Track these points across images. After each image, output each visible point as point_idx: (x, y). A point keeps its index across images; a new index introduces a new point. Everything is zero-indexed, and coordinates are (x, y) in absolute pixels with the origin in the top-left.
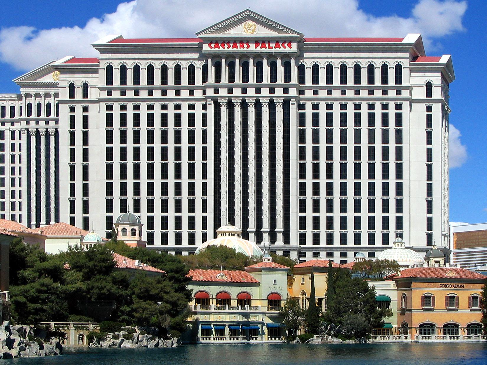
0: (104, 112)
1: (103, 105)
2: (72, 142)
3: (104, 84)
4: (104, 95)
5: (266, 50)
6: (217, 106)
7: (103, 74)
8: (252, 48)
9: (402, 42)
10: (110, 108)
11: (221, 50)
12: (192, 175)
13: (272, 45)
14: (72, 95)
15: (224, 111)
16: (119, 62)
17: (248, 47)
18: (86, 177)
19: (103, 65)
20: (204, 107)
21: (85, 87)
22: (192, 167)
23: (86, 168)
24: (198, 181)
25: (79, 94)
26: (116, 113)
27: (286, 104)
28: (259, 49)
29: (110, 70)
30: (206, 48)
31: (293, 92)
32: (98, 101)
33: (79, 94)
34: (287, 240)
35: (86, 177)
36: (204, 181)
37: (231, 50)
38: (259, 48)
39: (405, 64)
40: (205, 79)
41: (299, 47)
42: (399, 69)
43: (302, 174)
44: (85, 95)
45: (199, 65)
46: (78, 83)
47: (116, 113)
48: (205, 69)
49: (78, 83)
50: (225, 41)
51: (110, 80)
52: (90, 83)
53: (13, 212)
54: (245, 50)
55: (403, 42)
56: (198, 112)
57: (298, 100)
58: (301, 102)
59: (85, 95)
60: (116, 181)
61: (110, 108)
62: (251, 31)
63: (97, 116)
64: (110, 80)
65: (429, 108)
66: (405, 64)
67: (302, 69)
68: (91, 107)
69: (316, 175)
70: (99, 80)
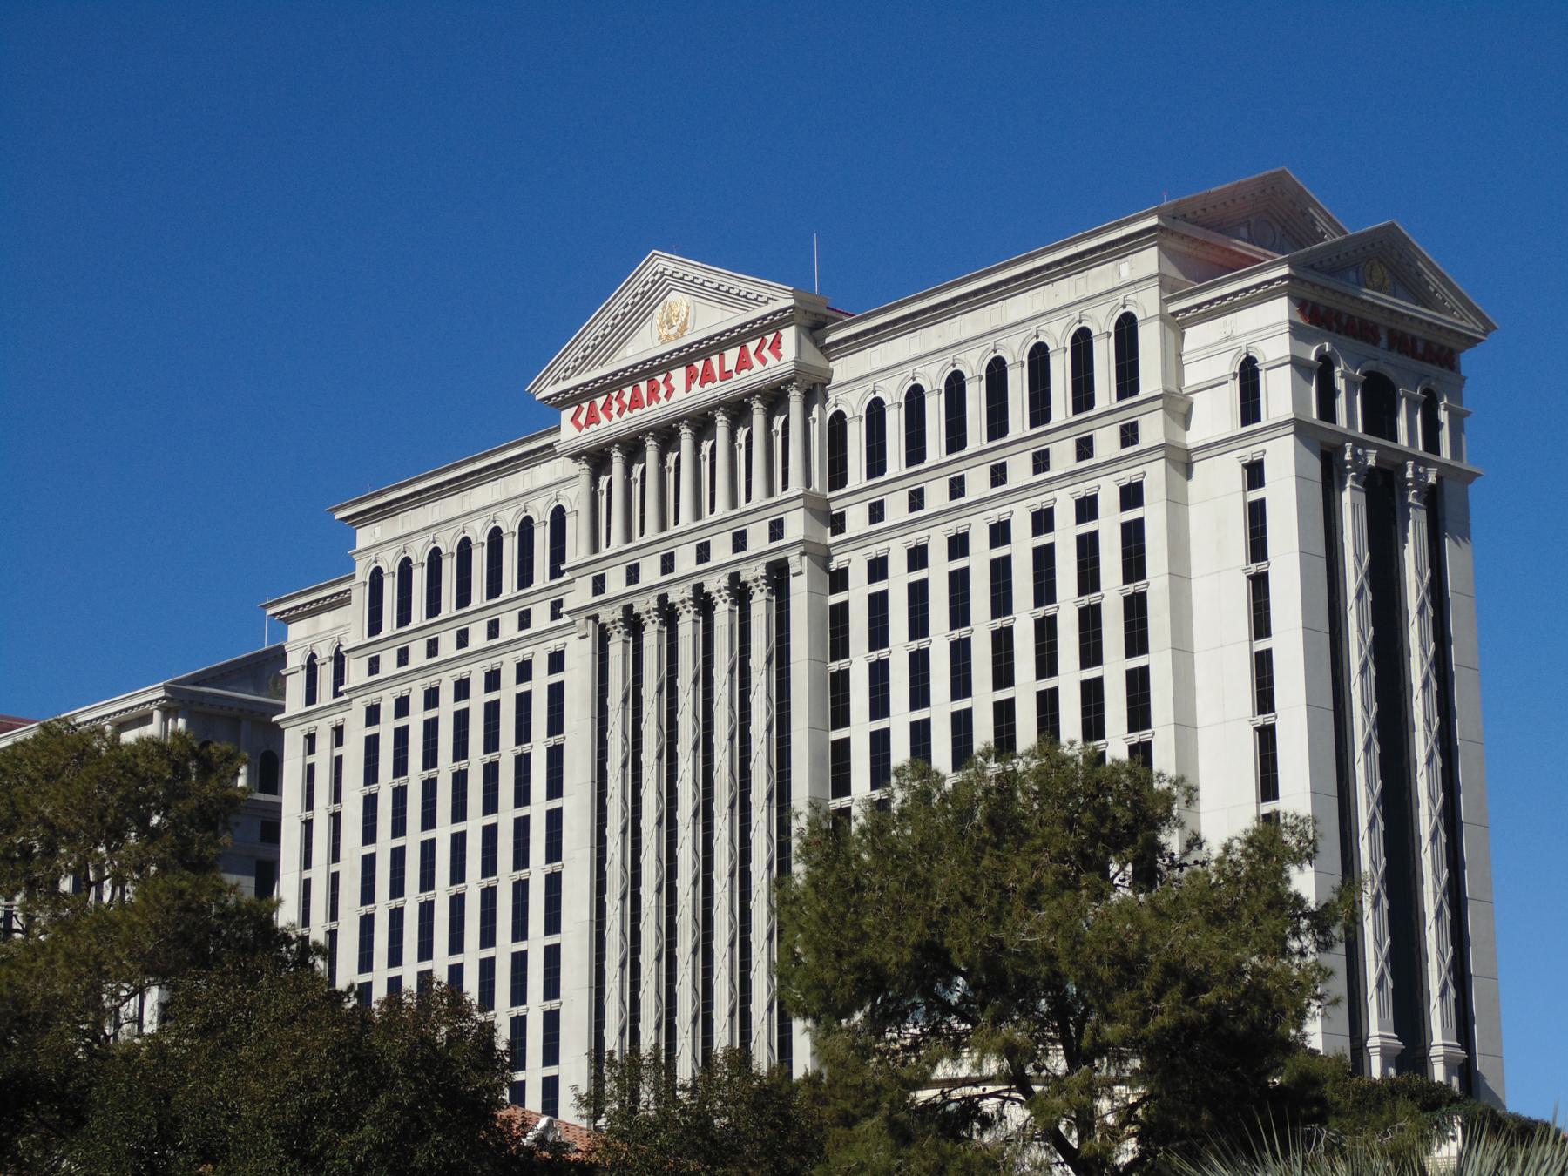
7: (361, 597)
19: (363, 573)
29: (377, 577)
38: (695, 387)
42: (1126, 329)
65: (1255, 474)
66: (1146, 304)
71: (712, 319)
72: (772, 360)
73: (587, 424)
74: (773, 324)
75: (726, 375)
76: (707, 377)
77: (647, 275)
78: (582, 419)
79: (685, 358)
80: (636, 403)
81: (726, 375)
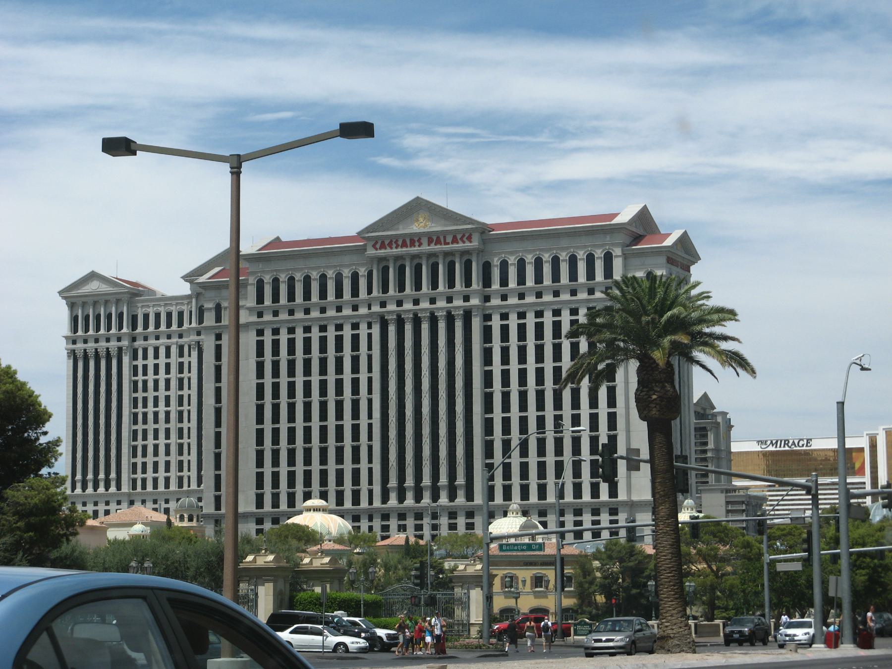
4: (254, 319)
8: (425, 248)
10: (260, 333)
11: (387, 251)
22: (356, 404)
24: (363, 422)
26: (268, 338)
27: (467, 316)
28: (434, 248)
31: (475, 301)
34: (470, 497)
36: (370, 421)
39: (617, 252)
41: (484, 242)
42: (608, 259)
43: (488, 406)
45: (362, 272)
47: (268, 338)
48: (370, 275)
50: (393, 241)
51: (260, 299)
54: (415, 249)
55: (617, 220)
66: (617, 252)
67: (487, 268)
69: (506, 407)
73: (380, 249)
75: (446, 243)
76: (438, 242)
78: (378, 246)
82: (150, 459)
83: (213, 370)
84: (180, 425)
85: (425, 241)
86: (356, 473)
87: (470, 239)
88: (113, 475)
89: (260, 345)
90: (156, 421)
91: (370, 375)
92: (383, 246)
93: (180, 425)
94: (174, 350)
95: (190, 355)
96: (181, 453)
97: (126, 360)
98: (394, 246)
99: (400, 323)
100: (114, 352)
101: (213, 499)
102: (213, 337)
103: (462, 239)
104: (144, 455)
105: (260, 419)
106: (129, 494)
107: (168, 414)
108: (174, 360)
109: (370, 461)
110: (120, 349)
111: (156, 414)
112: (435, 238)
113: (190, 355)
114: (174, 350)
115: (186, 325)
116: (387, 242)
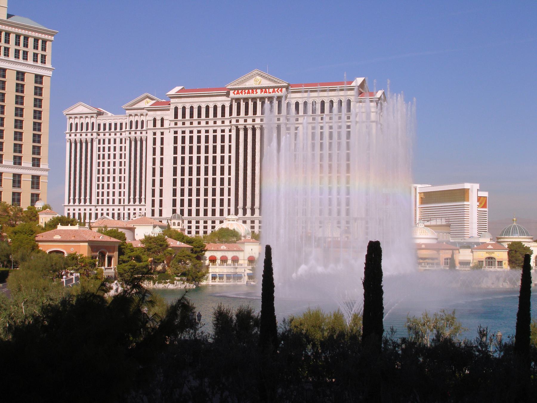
0: (173, 135)
1: (172, 131)
2: (154, 154)
3: (172, 118)
5: (267, 95)
6: (238, 130)
7: (172, 112)
8: (259, 94)
9: (351, 85)
10: (176, 132)
11: (240, 96)
12: (222, 173)
13: (271, 90)
14: (155, 125)
15: (242, 133)
16: (181, 104)
17: (257, 93)
18: (161, 175)
19: (172, 107)
20: (230, 131)
21: (162, 120)
22: (222, 168)
23: (162, 169)
24: (226, 177)
25: (158, 123)
26: (180, 136)
28: (263, 95)
29: (176, 109)
30: (232, 94)
32: (169, 128)
33: (158, 123)
35: (161, 175)
37: (246, 96)
38: (263, 93)
40: (231, 114)
42: (349, 102)
44: (162, 125)
45: (227, 105)
46: (158, 118)
47: (180, 136)
49: (158, 118)
51: (176, 116)
52: (165, 118)
53: (120, 197)
56: (227, 134)
57: (286, 124)
58: (288, 126)
59: (162, 125)
60: (179, 177)
61: (176, 132)
62: (258, 83)
63: (169, 137)
64: (176, 116)
66: (352, 99)
67: (288, 105)
68: (166, 132)
70: (169, 115)
71: (266, 83)
72: (280, 93)
74: (282, 87)
75: (269, 93)
76: (266, 92)
77: (254, 73)
78: (236, 93)
79: (261, 88)
80: (249, 93)
81: (269, 93)
82: (106, 190)
83: (160, 149)
84: (120, 175)
85: (259, 91)
86: (222, 201)
87: (281, 91)
88: (88, 197)
89: (176, 139)
90: (109, 173)
91: (230, 154)
92: (238, 93)
93: (120, 175)
94: (118, 141)
95: (125, 143)
96: (120, 188)
97: (95, 144)
98: (243, 93)
99: (246, 130)
100: (89, 141)
101: (151, 211)
102: (152, 134)
103: (277, 91)
104: (103, 188)
105: (175, 174)
106: (96, 206)
107: (114, 170)
108: (118, 145)
109: (229, 195)
110: (92, 139)
111: (109, 170)
112: (264, 90)
113: (125, 143)
114: (118, 141)
115: (124, 129)
116: (240, 91)
